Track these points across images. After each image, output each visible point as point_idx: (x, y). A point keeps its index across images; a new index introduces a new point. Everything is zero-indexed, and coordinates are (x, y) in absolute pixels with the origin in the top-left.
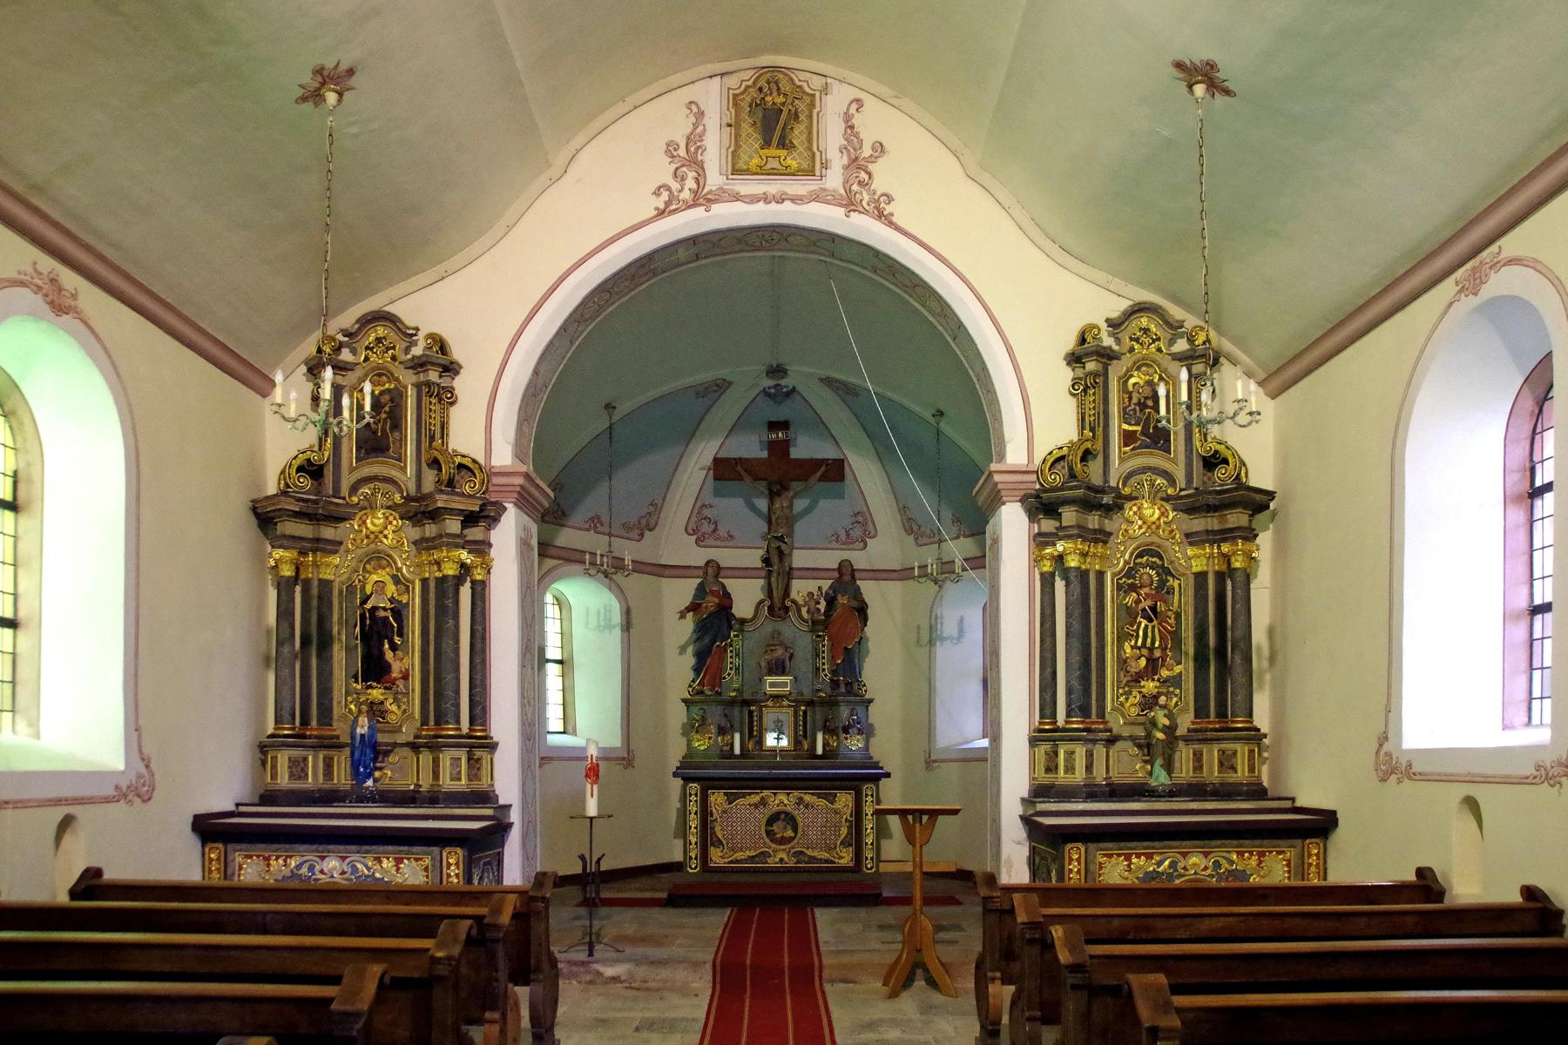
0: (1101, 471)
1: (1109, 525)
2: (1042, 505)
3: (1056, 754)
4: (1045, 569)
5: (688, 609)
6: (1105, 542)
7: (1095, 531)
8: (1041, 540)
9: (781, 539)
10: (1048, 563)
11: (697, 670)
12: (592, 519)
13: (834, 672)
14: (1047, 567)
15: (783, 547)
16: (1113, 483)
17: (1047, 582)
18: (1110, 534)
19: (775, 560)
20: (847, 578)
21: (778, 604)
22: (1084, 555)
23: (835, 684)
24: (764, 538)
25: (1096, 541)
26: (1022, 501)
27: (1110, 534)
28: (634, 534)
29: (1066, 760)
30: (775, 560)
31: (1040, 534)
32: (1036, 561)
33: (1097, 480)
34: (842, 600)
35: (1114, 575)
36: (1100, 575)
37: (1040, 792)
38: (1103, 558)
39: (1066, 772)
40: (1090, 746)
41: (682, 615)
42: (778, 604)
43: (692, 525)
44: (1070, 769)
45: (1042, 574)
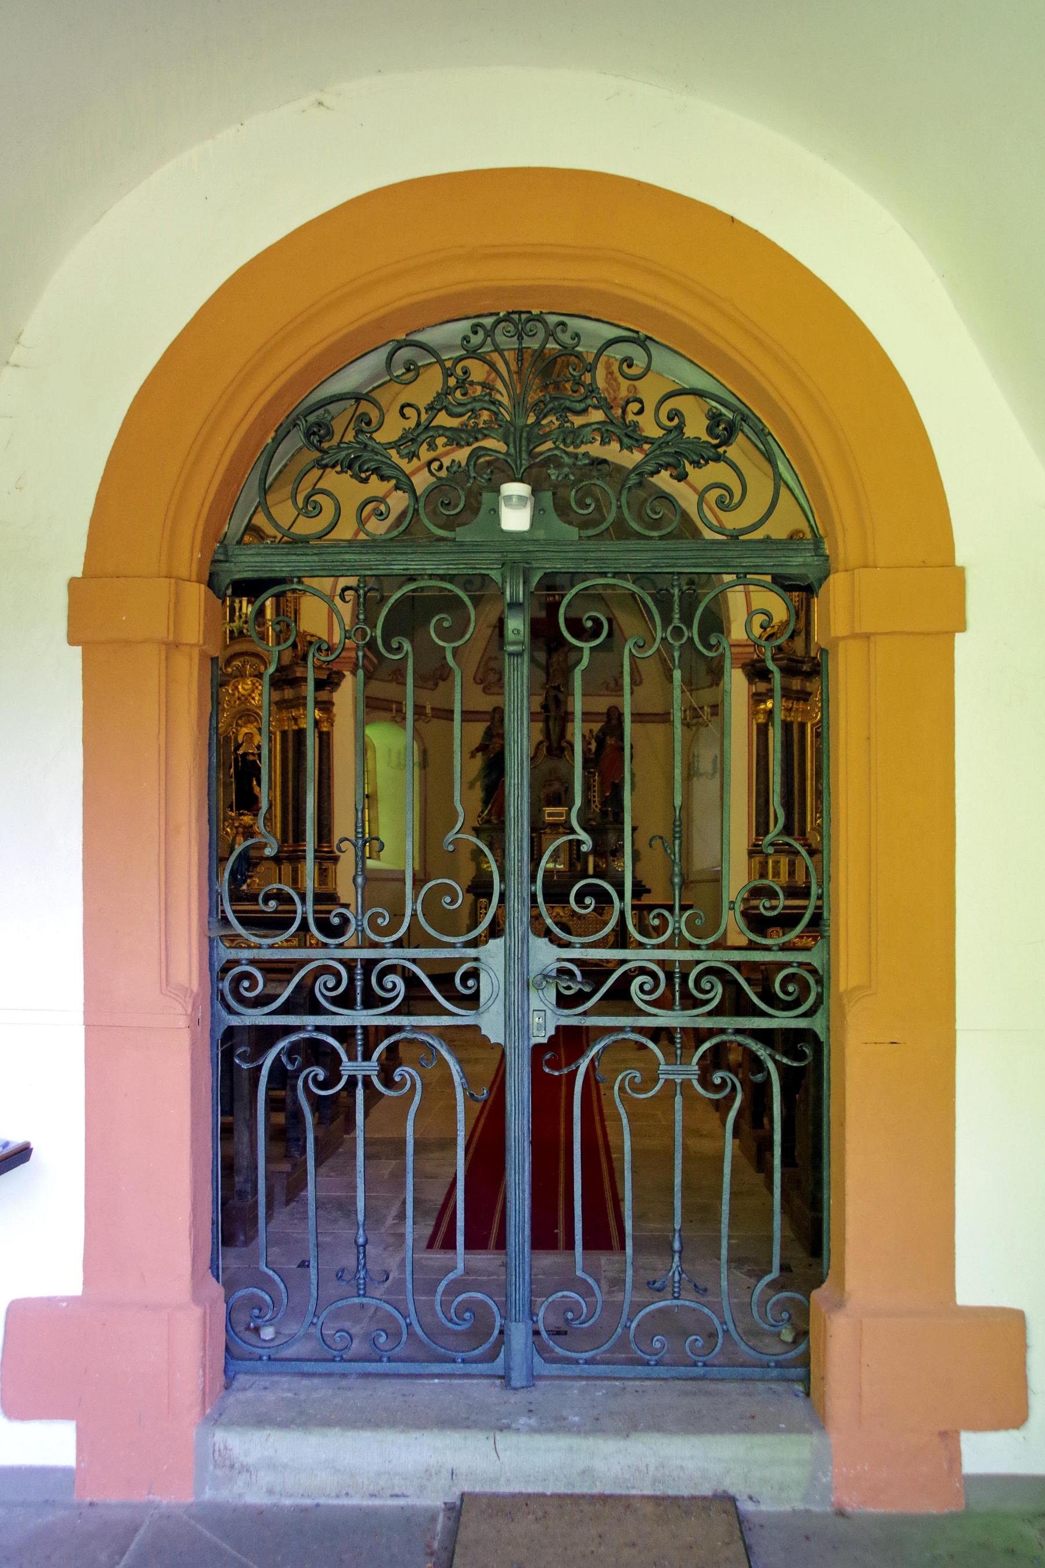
0: (803, 645)
1: (809, 687)
2: (756, 672)
3: (767, 863)
4: (760, 721)
5: (478, 750)
6: (806, 700)
7: (798, 692)
8: (758, 698)
9: (557, 688)
10: (762, 716)
11: (486, 802)
12: (394, 672)
13: (604, 803)
14: (761, 719)
15: (561, 696)
16: (813, 654)
17: (763, 731)
18: (810, 694)
19: (552, 707)
20: (614, 722)
21: (555, 745)
22: (789, 710)
23: (604, 813)
24: (543, 687)
25: (798, 699)
26: (744, 667)
27: (810, 694)
28: (431, 684)
29: (773, 867)
30: (552, 707)
31: (755, 694)
32: (753, 713)
33: (800, 651)
34: (610, 741)
35: (813, 726)
36: (802, 726)
37: (756, 892)
38: (805, 712)
39: (773, 877)
40: (793, 857)
41: (473, 755)
42: (555, 745)
43: (480, 676)
44: (777, 874)
45: (758, 725)
